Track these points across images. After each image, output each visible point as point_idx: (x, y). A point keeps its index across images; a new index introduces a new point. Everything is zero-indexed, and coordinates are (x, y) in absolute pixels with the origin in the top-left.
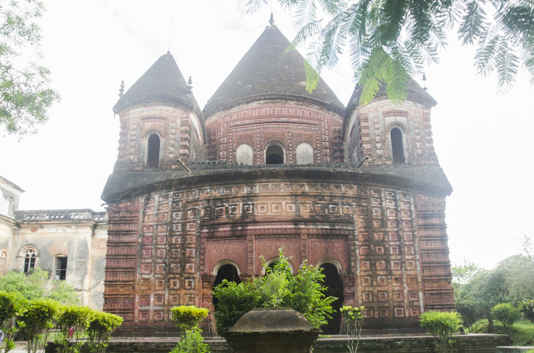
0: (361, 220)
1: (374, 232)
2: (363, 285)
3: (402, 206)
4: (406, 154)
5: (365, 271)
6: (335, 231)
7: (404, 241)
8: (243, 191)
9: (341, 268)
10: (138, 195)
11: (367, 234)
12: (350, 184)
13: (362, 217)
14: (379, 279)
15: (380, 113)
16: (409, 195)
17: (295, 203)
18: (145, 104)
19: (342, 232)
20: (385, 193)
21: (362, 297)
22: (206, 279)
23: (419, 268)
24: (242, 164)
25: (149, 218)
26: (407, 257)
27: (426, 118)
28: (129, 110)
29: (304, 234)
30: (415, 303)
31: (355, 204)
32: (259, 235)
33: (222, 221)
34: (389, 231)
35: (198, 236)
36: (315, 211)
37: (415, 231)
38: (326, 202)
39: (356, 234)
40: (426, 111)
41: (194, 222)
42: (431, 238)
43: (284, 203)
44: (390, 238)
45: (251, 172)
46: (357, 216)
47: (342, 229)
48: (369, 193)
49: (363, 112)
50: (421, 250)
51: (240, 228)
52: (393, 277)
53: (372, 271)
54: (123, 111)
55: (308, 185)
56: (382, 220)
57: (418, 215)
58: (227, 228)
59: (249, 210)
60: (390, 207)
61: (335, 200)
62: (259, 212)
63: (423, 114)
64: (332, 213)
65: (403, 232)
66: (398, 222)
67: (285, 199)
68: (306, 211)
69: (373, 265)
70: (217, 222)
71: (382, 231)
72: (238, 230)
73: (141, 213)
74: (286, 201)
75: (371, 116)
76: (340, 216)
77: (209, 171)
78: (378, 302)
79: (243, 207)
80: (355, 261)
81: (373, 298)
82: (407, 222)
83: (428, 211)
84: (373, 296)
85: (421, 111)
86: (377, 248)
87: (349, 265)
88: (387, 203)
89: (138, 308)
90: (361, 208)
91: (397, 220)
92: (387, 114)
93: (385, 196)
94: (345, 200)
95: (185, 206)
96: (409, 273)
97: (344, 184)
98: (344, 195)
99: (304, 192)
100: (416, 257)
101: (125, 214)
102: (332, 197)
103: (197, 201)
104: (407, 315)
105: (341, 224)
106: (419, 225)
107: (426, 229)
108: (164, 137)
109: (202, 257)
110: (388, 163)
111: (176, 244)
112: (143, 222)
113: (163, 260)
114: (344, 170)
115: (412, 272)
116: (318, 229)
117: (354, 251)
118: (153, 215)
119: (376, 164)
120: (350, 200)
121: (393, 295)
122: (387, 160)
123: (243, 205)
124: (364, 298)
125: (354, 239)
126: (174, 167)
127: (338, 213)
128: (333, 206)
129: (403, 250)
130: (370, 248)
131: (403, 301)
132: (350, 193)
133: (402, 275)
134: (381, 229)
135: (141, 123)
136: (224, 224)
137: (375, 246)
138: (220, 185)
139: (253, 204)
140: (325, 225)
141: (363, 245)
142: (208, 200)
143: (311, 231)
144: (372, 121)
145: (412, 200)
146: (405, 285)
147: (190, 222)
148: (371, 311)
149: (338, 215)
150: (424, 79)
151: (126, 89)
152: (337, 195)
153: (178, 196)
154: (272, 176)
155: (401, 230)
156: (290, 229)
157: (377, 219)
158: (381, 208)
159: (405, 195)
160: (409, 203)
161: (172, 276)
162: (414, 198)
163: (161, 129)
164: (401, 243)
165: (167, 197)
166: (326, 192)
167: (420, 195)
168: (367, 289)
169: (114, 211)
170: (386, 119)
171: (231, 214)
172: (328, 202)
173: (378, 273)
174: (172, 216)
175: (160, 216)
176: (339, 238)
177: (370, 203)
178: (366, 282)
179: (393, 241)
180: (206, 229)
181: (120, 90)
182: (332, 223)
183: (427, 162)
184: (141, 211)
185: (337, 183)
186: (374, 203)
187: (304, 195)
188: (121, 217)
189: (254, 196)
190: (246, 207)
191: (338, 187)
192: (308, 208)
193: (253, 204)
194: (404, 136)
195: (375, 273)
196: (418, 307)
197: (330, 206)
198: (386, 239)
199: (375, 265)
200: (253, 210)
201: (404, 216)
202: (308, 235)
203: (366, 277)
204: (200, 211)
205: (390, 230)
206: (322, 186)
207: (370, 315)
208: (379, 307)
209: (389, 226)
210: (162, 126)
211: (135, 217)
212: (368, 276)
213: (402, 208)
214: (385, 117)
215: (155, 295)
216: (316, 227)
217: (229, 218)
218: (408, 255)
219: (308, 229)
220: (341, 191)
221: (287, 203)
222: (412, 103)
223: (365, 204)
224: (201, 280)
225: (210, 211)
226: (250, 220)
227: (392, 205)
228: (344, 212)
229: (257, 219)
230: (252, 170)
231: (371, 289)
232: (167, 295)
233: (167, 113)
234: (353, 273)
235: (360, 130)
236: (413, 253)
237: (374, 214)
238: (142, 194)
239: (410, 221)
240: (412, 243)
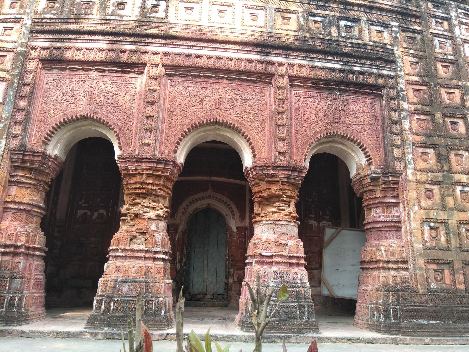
0: (410, 58)
1: (441, 86)
2: (423, 204)
5: (427, 171)
9: (364, 161)
11: (424, 88)
13: (412, 52)
14: (458, 192)
19: (371, 80)
21: (423, 233)
22: (23, 161)
31: (397, 24)
35: (20, 54)
36: (309, 30)
38: (332, 13)
39: (401, 86)
46: (402, 49)
47: (371, 74)
48: (424, 6)
53: (443, 171)
59: (156, 12)
61: (351, 13)
64: (346, 38)
68: (289, 27)
69: (442, 159)
71: (457, 87)
72: (124, 51)
80: (402, 146)
81: (448, 239)
84: (447, 233)
86: (448, 120)
90: (409, 34)
94: (374, 16)
109: (23, 104)
116: (313, 68)
120: (385, 18)
124: (427, 235)
125: (397, 97)
127: (360, 39)
128: (349, 24)
130: (434, 120)
134: (454, 82)
137: (445, 116)
141: (416, 112)
143: (296, 71)
148: (446, 272)
149: (360, 42)
156: (250, 61)
157: (445, 61)
158: (452, 38)
168: (433, 215)
172: (337, 14)
173: (457, 177)
176: (362, 93)
177: (428, 27)
178: (429, 198)
180: (45, 39)
195: (451, 178)
197: (343, 23)
199: (448, 159)
200: (167, 11)
202: (292, 78)
203: (429, 187)
207: (442, 280)
212: (434, 183)
216: (311, 63)
219: (292, 65)
223: (418, 28)
226: (155, 32)
228: (373, 39)
231: (442, 215)
234: (396, 174)
237: (438, 50)
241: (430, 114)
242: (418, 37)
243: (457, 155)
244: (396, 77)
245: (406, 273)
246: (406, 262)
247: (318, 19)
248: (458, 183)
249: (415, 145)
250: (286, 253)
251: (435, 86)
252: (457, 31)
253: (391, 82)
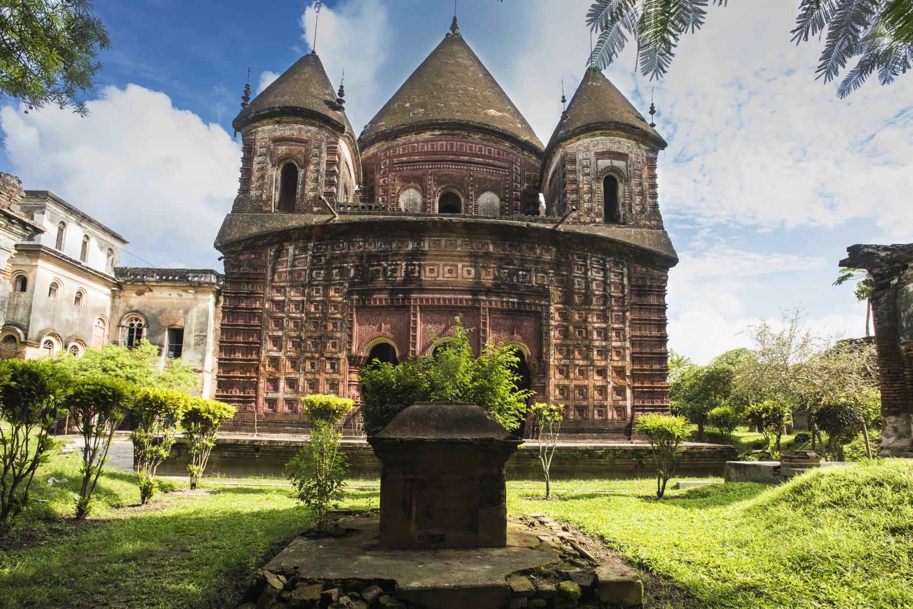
3: (613, 278)
4: (621, 210)
8: (407, 246)
10: (266, 246)
12: (548, 245)
15: (593, 153)
16: (623, 264)
17: (475, 267)
18: (278, 119)
20: (592, 261)
23: (628, 358)
24: (406, 210)
25: (280, 277)
26: (614, 344)
27: (651, 163)
28: (256, 127)
30: (621, 403)
33: (379, 286)
36: (501, 279)
37: (627, 311)
39: (552, 311)
40: (651, 155)
41: (341, 284)
43: (460, 266)
45: (420, 222)
49: (570, 151)
54: (248, 128)
55: (492, 243)
56: (584, 294)
58: (384, 296)
62: (427, 276)
63: (648, 159)
65: (612, 311)
66: (606, 298)
67: (461, 261)
70: (371, 286)
73: (269, 270)
75: (580, 157)
76: (533, 286)
77: (363, 217)
79: (407, 268)
82: (617, 299)
83: (645, 286)
85: (645, 154)
87: (541, 350)
89: (262, 395)
92: (601, 155)
93: (591, 263)
95: (329, 263)
96: (615, 364)
101: (248, 270)
102: (523, 261)
103: (344, 256)
104: (610, 417)
108: (303, 167)
111: (315, 313)
112: (272, 281)
113: (297, 333)
114: (542, 225)
115: (620, 364)
117: (548, 333)
118: (286, 272)
119: (582, 220)
120: (547, 267)
123: (407, 265)
126: (315, 209)
133: (606, 366)
135: (272, 146)
138: (376, 237)
139: (420, 265)
142: (360, 257)
144: (580, 163)
145: (625, 270)
146: (609, 380)
147: (335, 284)
150: (652, 111)
151: (252, 98)
153: (320, 249)
154: (447, 228)
158: (586, 278)
160: (622, 274)
161: (309, 355)
162: (628, 269)
163: (299, 156)
164: (609, 326)
168: (562, 382)
169: (232, 265)
170: (600, 162)
171: (391, 276)
173: (577, 362)
174: (311, 275)
175: (295, 275)
177: (571, 272)
181: (243, 98)
182: (521, 296)
183: (647, 223)
184: (270, 266)
186: (577, 273)
187: (487, 255)
188: (241, 274)
189: (422, 255)
190: (409, 267)
191: (532, 249)
192: (491, 273)
193: (420, 265)
194: (621, 187)
196: (624, 408)
198: (590, 320)
199: (573, 352)
200: (419, 272)
201: (614, 291)
204: (349, 271)
205: (595, 307)
206: (511, 246)
209: (594, 302)
210: (301, 151)
211: (261, 274)
214: (597, 159)
215: (287, 379)
217: (387, 281)
218: (616, 341)
220: (535, 253)
221: (463, 266)
222: (634, 142)
224: (347, 362)
225: (362, 271)
227: (599, 277)
230: (420, 218)
231: (566, 382)
232: (302, 380)
233: (309, 134)
235: (564, 175)
238: (271, 244)
239: (621, 298)
244: (548, 306)
248: (577, 365)
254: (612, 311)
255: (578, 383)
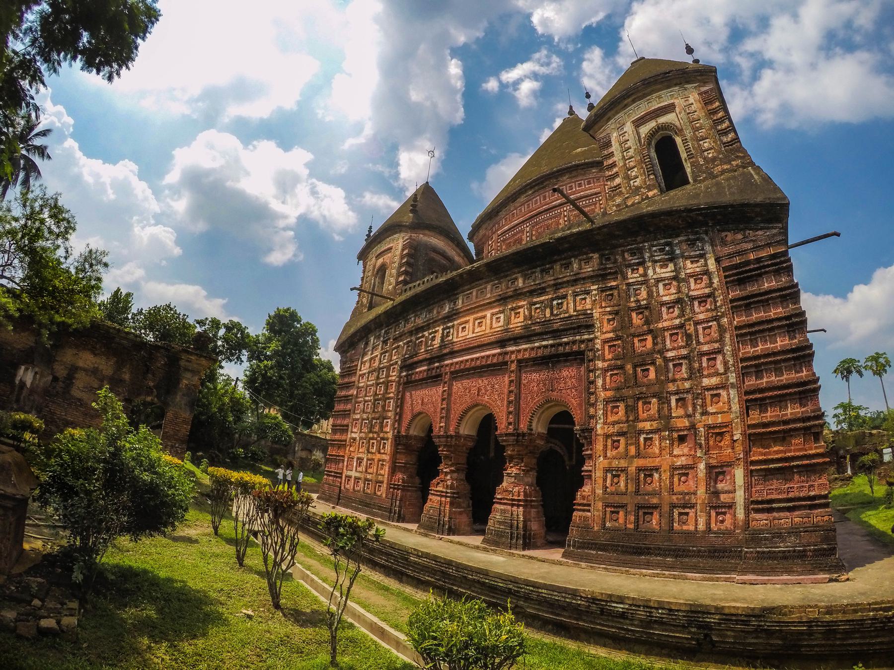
1: (634, 336)
5: (614, 423)
6: (562, 348)
7: (698, 343)
12: (587, 254)
13: (608, 309)
14: (642, 439)
21: (605, 480)
26: (706, 382)
29: (512, 362)
31: (596, 287)
32: (456, 372)
33: (421, 358)
34: (665, 329)
37: (722, 316)
39: (598, 346)
42: (761, 328)
44: (668, 342)
47: (574, 342)
50: (742, 360)
51: (437, 364)
52: (675, 435)
53: (627, 421)
57: (726, 277)
60: (663, 275)
65: (697, 323)
69: (631, 409)
70: (416, 359)
71: (650, 331)
74: (491, 311)
76: (571, 316)
78: (637, 492)
82: (702, 299)
86: (639, 370)
88: (658, 270)
91: (679, 301)
96: (710, 421)
97: (576, 257)
98: (578, 276)
99: (516, 290)
100: (727, 379)
105: (572, 332)
106: (732, 301)
107: (748, 307)
110: (650, 194)
115: (720, 419)
121: (672, 476)
122: (650, 190)
124: (609, 481)
129: (696, 365)
131: (695, 494)
132: (588, 269)
136: (421, 361)
140: (544, 340)
149: (566, 315)
152: (565, 279)
155: (689, 320)
156: (494, 355)
159: (692, 244)
165: (378, 337)
166: (549, 279)
167: (724, 234)
168: (615, 463)
173: (641, 425)
179: (674, 349)
185: (565, 259)
191: (568, 266)
195: (635, 427)
197: (555, 302)
202: (519, 361)
205: (666, 324)
206: (542, 271)
208: (639, 507)
209: (665, 316)
213: (688, 271)
218: (709, 376)
223: (614, 284)
228: (578, 308)
229: (456, 348)
231: (623, 463)
236: (722, 370)
239: (709, 296)
240: (716, 345)
241: (622, 367)
242: (615, 293)
243: (644, 403)
245: (589, 514)
246: (589, 505)
247: (538, 306)
248: (641, 432)
249: (607, 401)
250: (510, 497)
251: (628, 337)
252: (650, 272)
253: (590, 344)
254: (697, 323)
255: (641, 462)
